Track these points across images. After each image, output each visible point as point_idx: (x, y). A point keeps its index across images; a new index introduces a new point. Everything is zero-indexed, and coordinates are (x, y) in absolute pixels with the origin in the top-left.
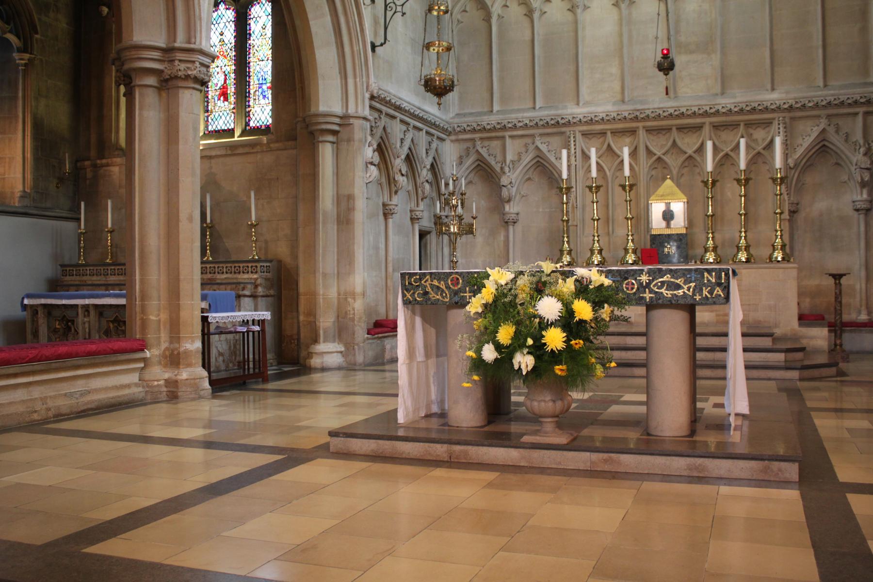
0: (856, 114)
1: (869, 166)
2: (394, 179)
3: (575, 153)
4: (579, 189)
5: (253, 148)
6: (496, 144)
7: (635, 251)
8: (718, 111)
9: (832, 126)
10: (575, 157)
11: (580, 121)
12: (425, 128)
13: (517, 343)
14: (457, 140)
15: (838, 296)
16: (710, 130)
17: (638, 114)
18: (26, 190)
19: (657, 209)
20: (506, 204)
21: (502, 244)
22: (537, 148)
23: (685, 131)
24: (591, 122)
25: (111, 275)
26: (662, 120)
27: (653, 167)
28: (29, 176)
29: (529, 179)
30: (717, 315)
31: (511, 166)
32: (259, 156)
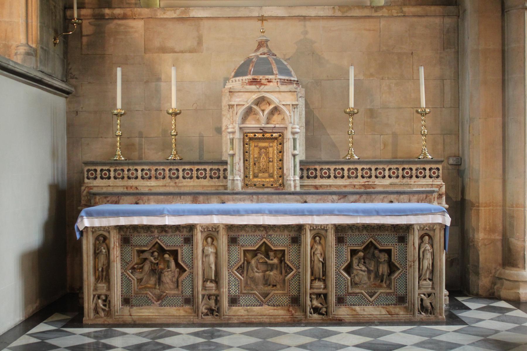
5: (376, 11)
18: (30, 43)
25: (184, 178)
28: (35, 22)
32: (383, 22)
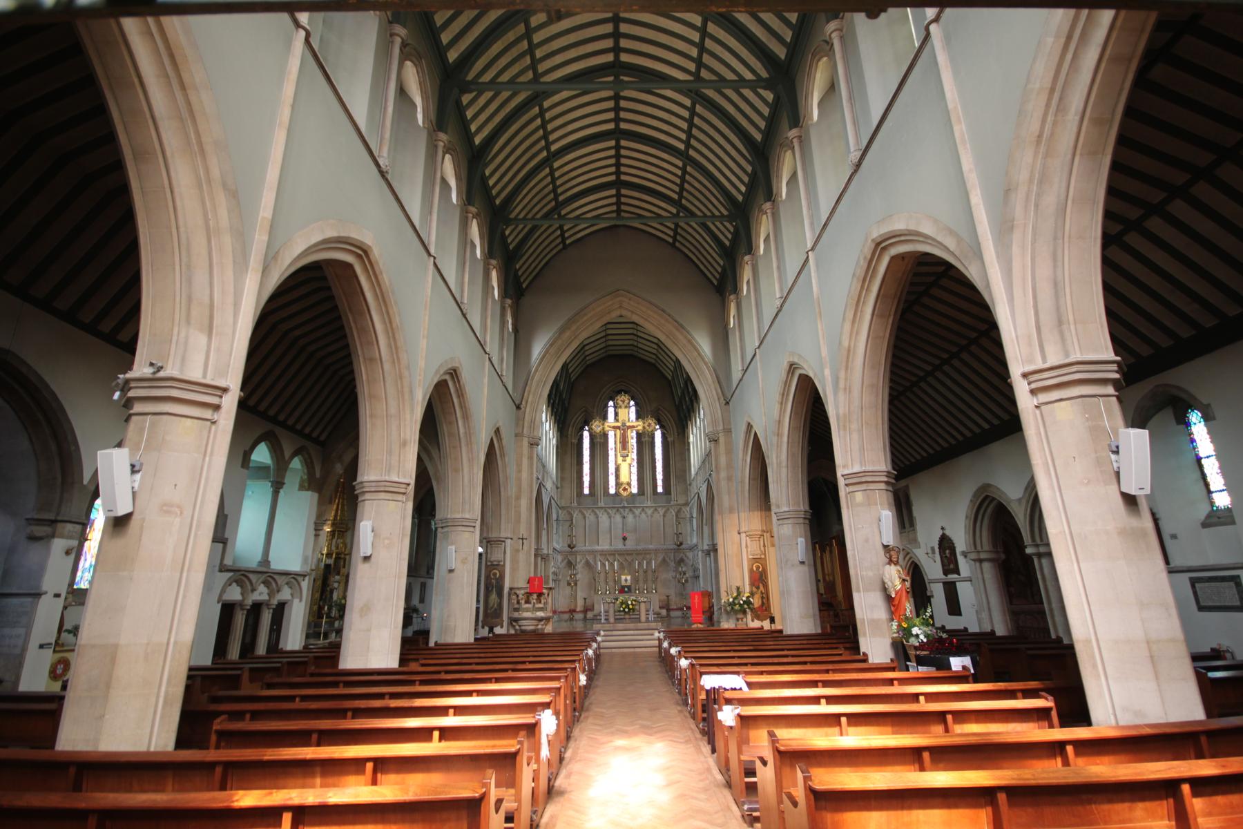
13: (626, 607)
15: (668, 601)
19: (623, 577)
24: (603, 551)
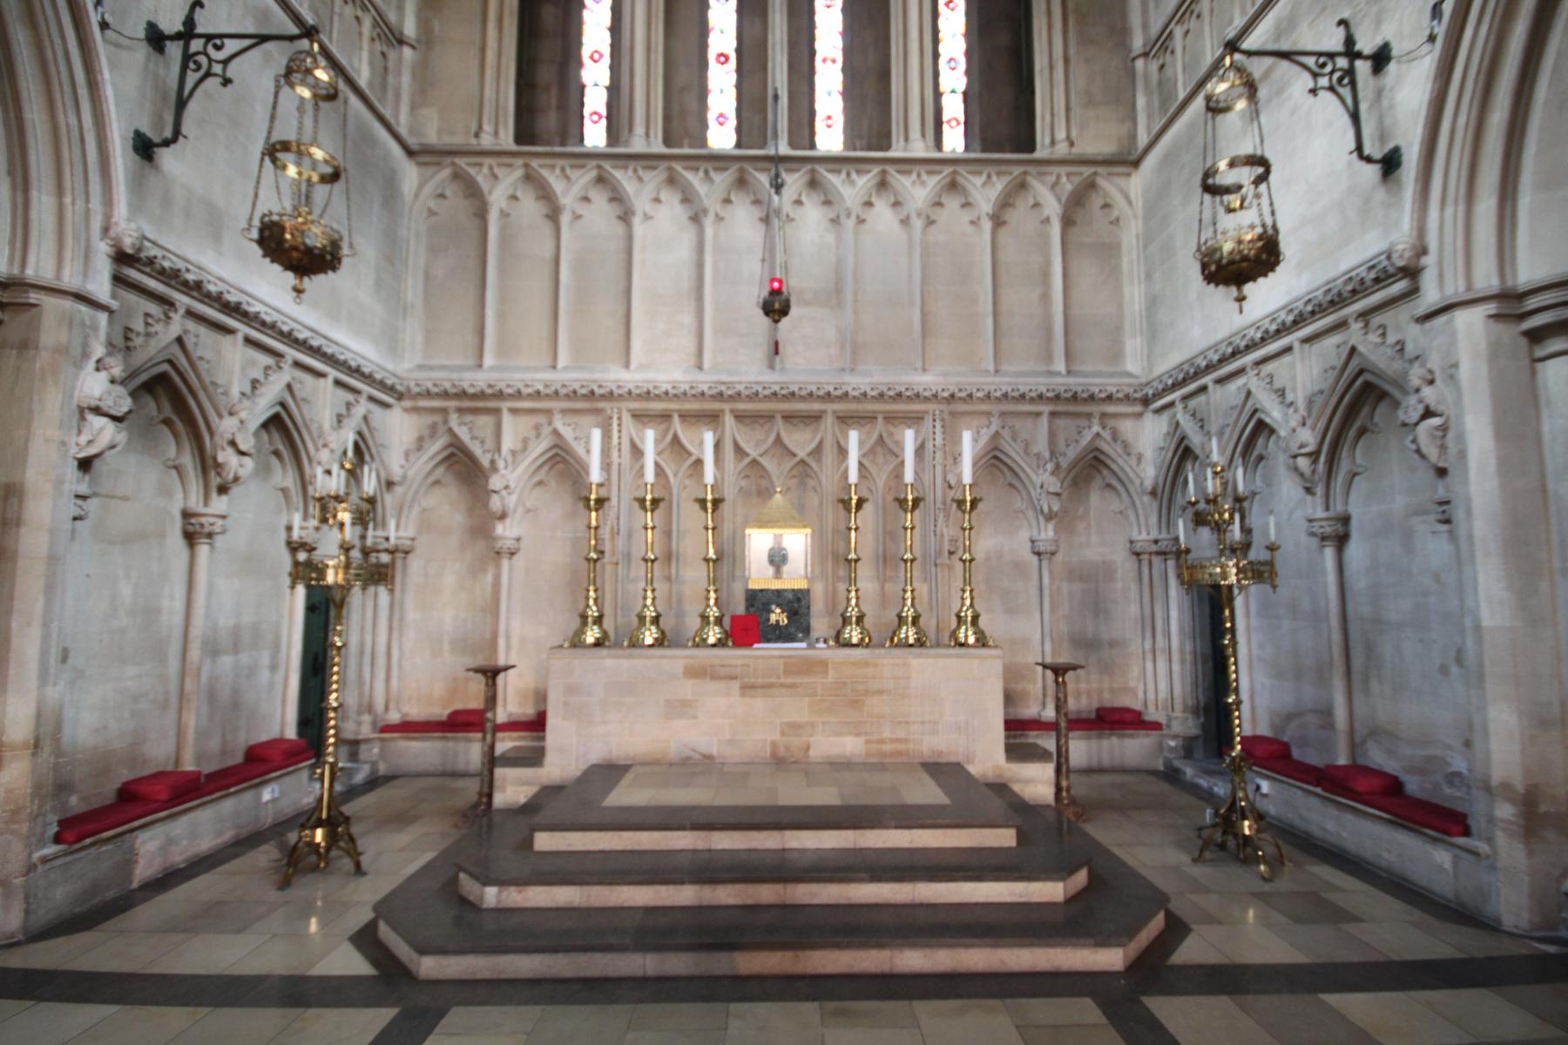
0: (1039, 414)
1: (1059, 491)
2: (215, 459)
3: (620, 444)
4: (621, 502)
6: (485, 421)
7: (719, 621)
8: (846, 394)
9: (1007, 428)
10: (620, 450)
11: (630, 393)
12: (333, 373)
14: (416, 410)
16: (833, 423)
17: (723, 388)
19: (759, 542)
20: (497, 522)
21: (489, 589)
22: (556, 433)
23: (795, 421)
24: (647, 396)
26: (761, 401)
27: (742, 475)
29: (540, 483)
30: (867, 742)
31: (510, 459)
